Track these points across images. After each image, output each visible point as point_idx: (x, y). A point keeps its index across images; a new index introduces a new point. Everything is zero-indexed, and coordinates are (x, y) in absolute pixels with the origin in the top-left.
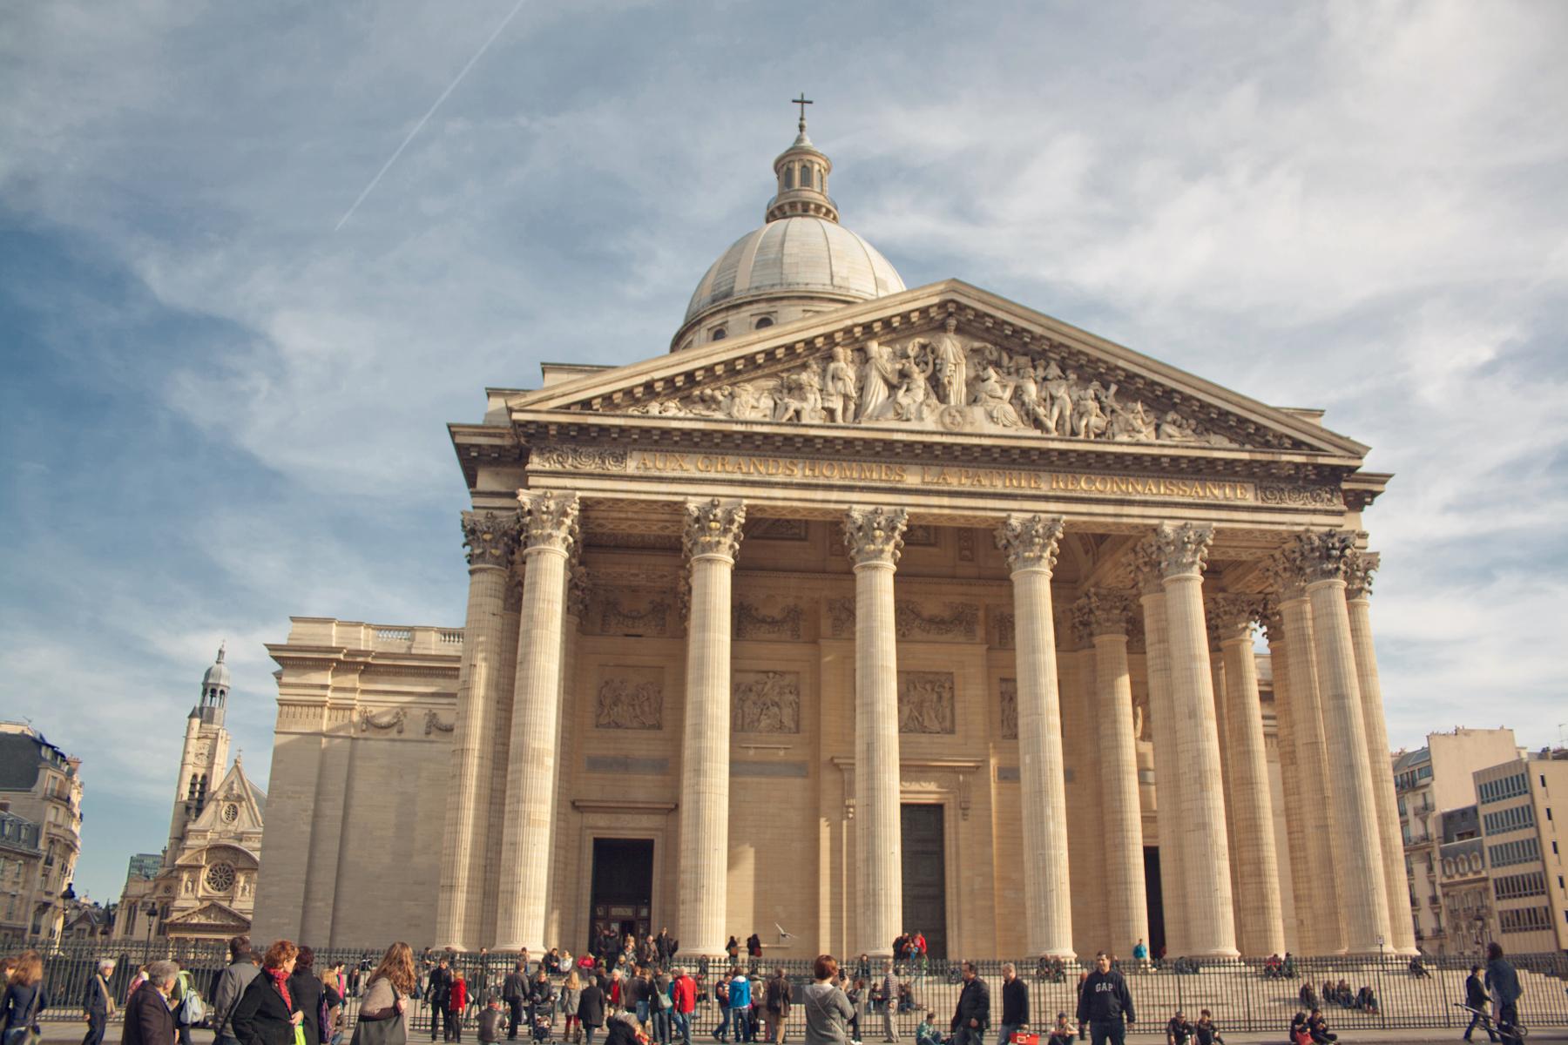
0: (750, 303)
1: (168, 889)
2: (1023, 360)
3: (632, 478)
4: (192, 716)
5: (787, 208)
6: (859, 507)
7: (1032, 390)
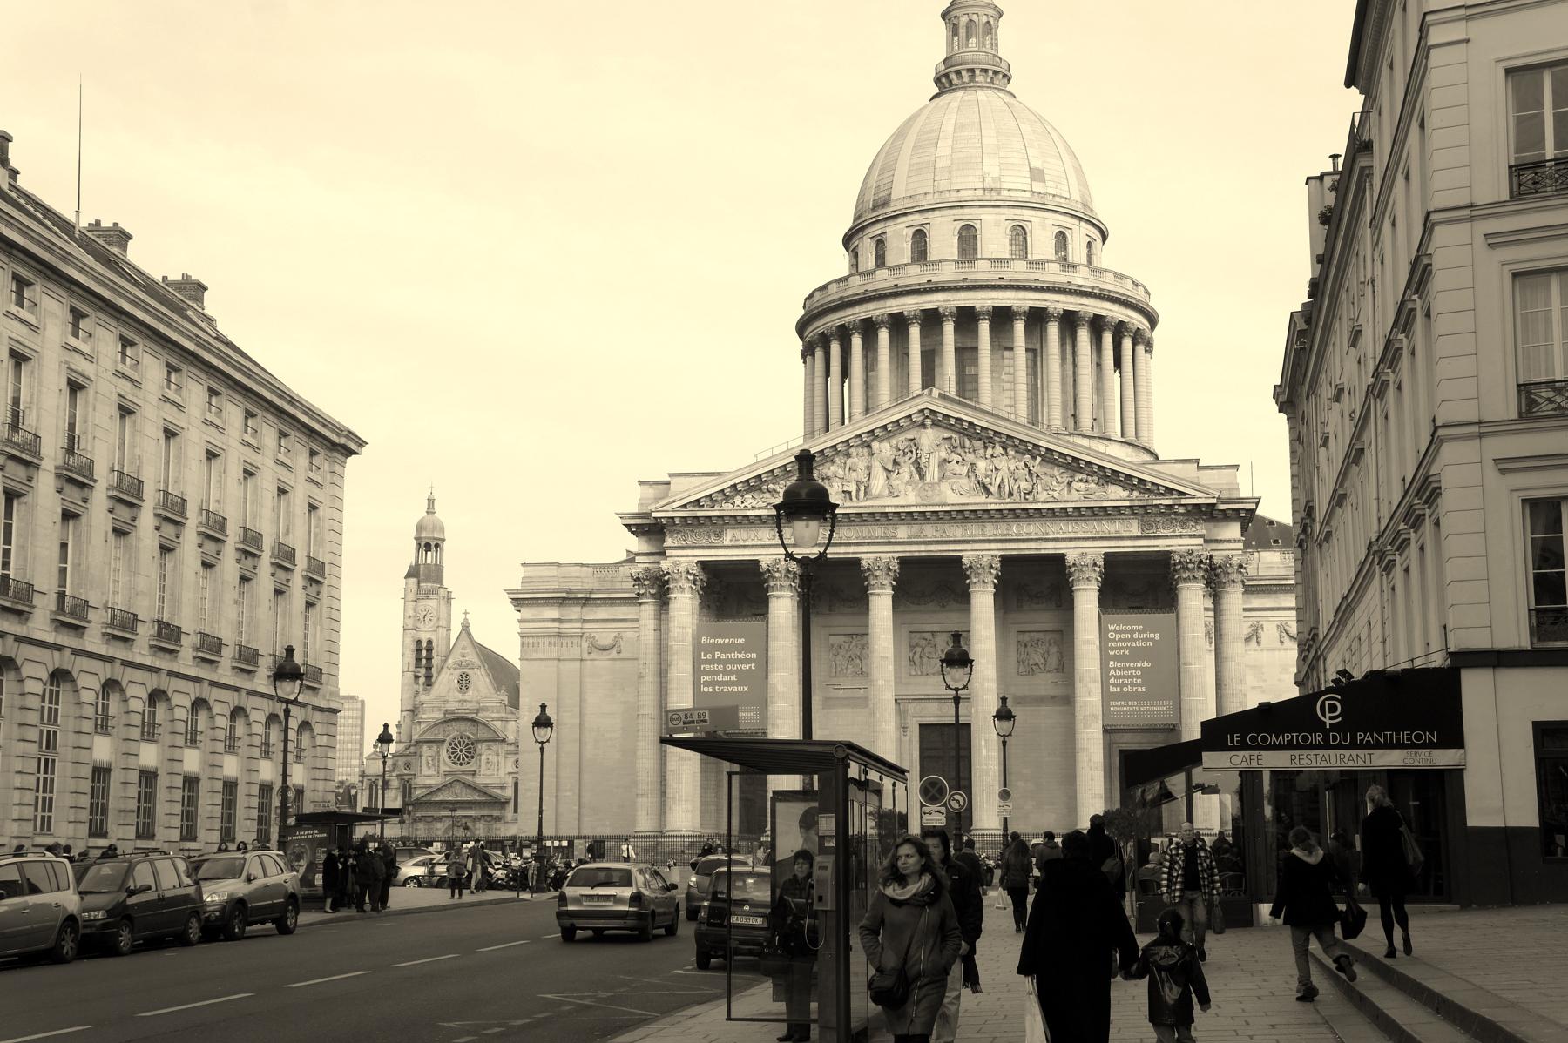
0: (905, 214)
1: (408, 765)
2: (978, 444)
3: (727, 547)
4: (408, 576)
5: (953, 76)
6: (867, 555)
7: (982, 466)
